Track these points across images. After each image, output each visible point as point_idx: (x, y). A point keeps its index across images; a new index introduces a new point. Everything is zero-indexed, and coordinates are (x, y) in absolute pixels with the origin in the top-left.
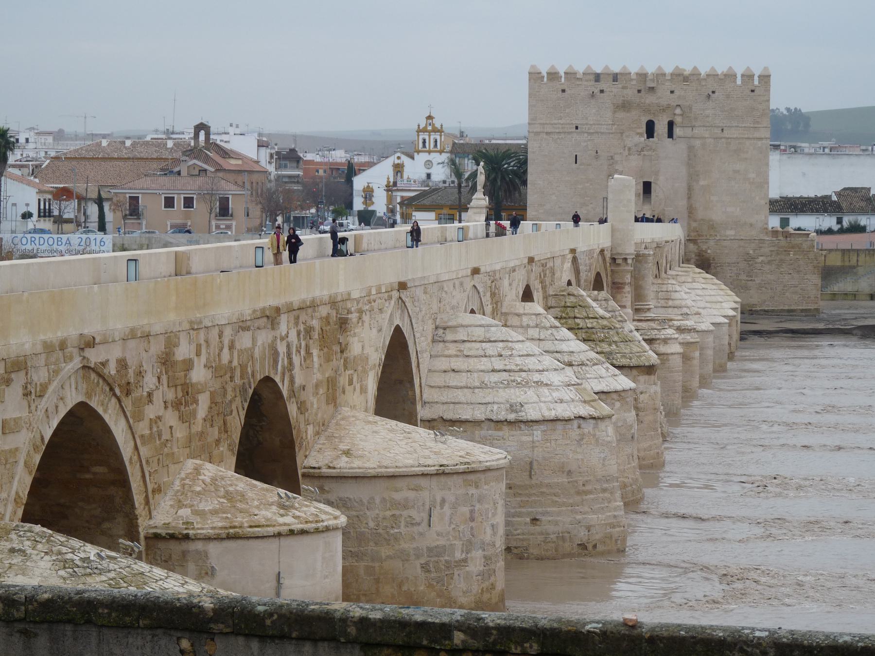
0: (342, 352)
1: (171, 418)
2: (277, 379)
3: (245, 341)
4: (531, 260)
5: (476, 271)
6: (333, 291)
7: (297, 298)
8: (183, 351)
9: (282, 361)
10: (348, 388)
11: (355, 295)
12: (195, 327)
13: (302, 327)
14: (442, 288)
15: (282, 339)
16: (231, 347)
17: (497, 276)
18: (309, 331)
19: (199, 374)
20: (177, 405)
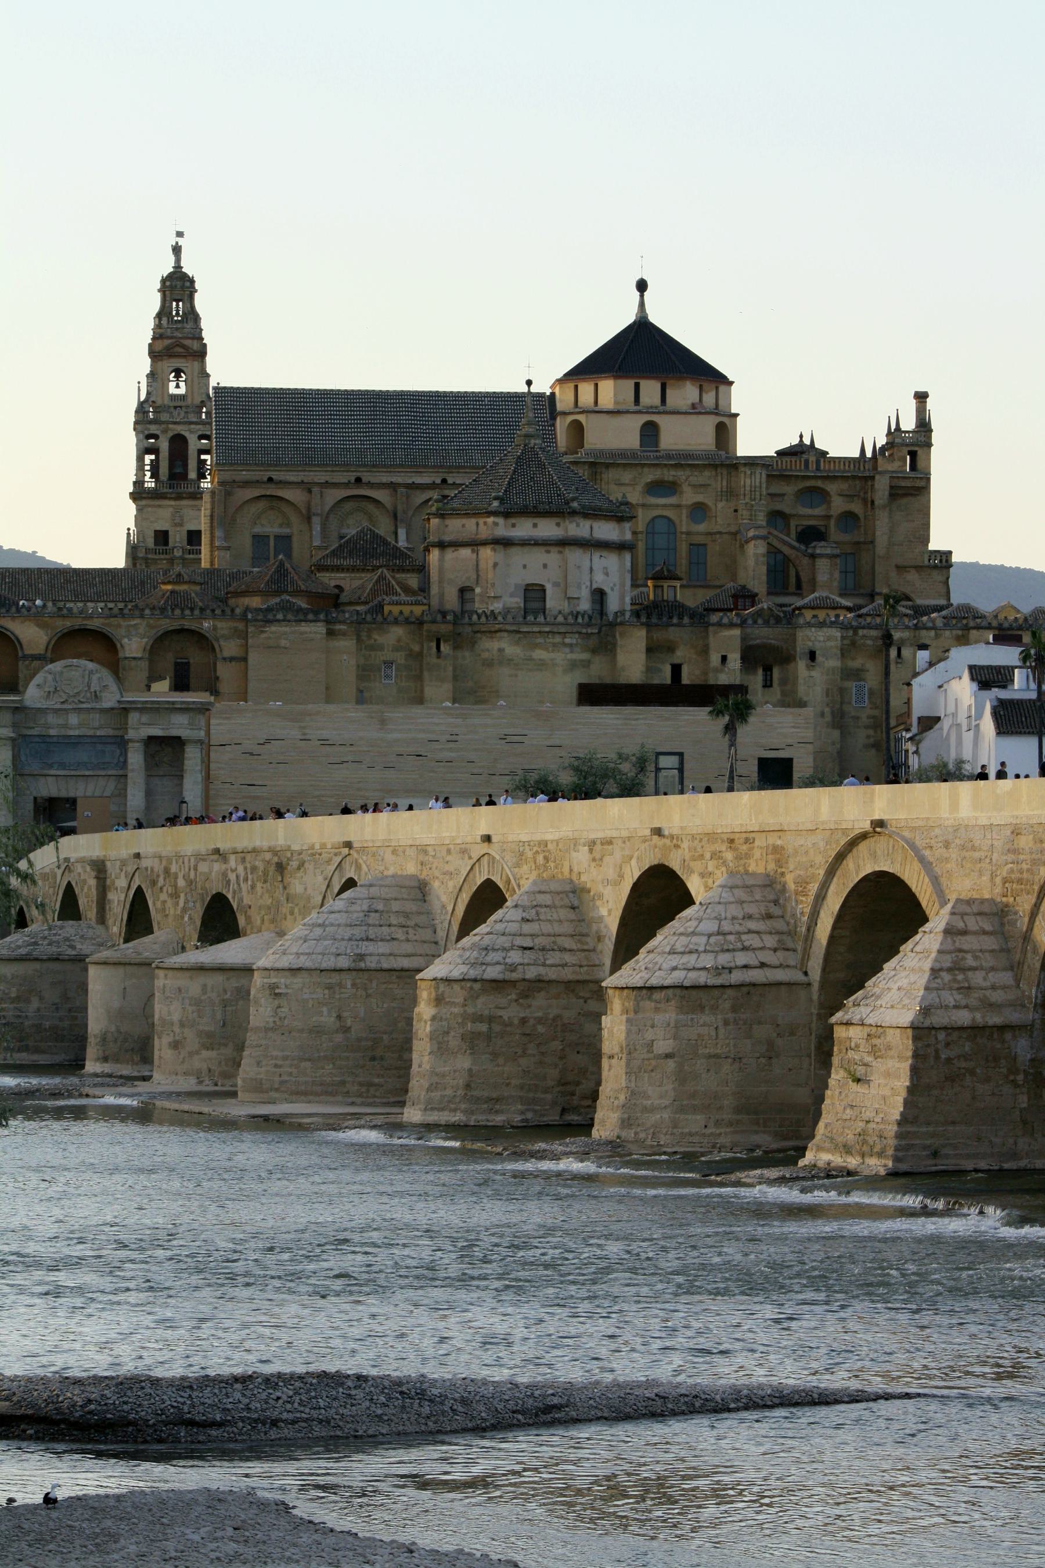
0: (285, 888)
1: (169, 903)
2: (230, 896)
3: (203, 867)
4: (658, 832)
5: (487, 839)
6: (273, 843)
7: (240, 846)
8: (174, 869)
9: (233, 885)
10: (289, 917)
11: (296, 847)
12: (179, 856)
13: (248, 866)
14: (426, 852)
15: (233, 871)
16: (196, 869)
17: (550, 846)
18: (254, 869)
19: (181, 883)
20: (171, 896)
